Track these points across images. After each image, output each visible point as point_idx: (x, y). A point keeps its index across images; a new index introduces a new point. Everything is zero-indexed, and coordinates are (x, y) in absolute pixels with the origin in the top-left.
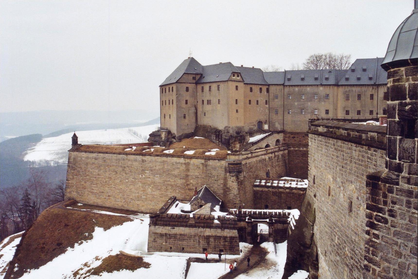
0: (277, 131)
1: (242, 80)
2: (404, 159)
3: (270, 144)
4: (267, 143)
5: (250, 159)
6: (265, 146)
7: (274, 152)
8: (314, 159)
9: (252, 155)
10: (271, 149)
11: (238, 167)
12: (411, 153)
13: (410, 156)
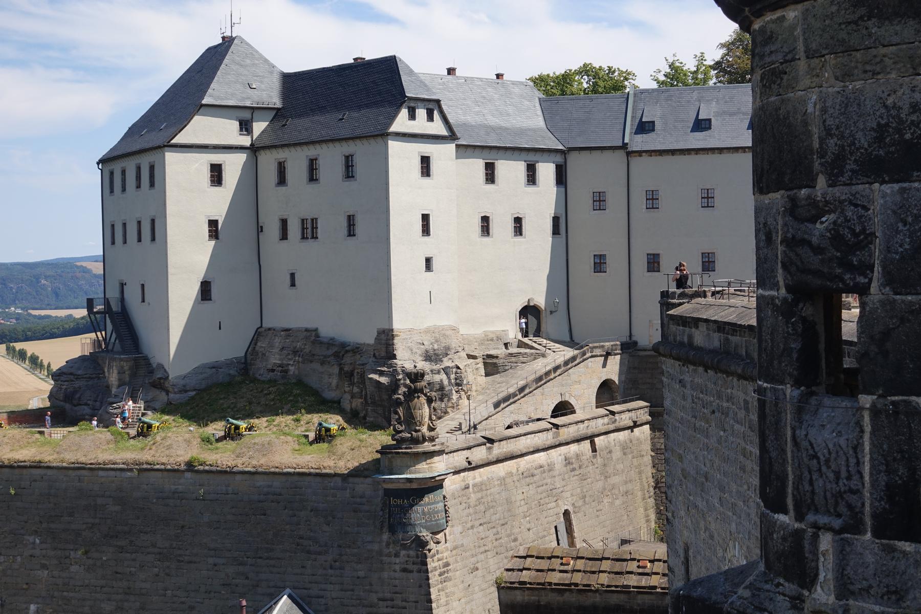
1: (444, 132)
2: (817, 511)
6: (553, 412)
7: (591, 438)
8: (683, 470)
9: (490, 448)
10: (577, 423)
12: (844, 474)
13: (840, 495)
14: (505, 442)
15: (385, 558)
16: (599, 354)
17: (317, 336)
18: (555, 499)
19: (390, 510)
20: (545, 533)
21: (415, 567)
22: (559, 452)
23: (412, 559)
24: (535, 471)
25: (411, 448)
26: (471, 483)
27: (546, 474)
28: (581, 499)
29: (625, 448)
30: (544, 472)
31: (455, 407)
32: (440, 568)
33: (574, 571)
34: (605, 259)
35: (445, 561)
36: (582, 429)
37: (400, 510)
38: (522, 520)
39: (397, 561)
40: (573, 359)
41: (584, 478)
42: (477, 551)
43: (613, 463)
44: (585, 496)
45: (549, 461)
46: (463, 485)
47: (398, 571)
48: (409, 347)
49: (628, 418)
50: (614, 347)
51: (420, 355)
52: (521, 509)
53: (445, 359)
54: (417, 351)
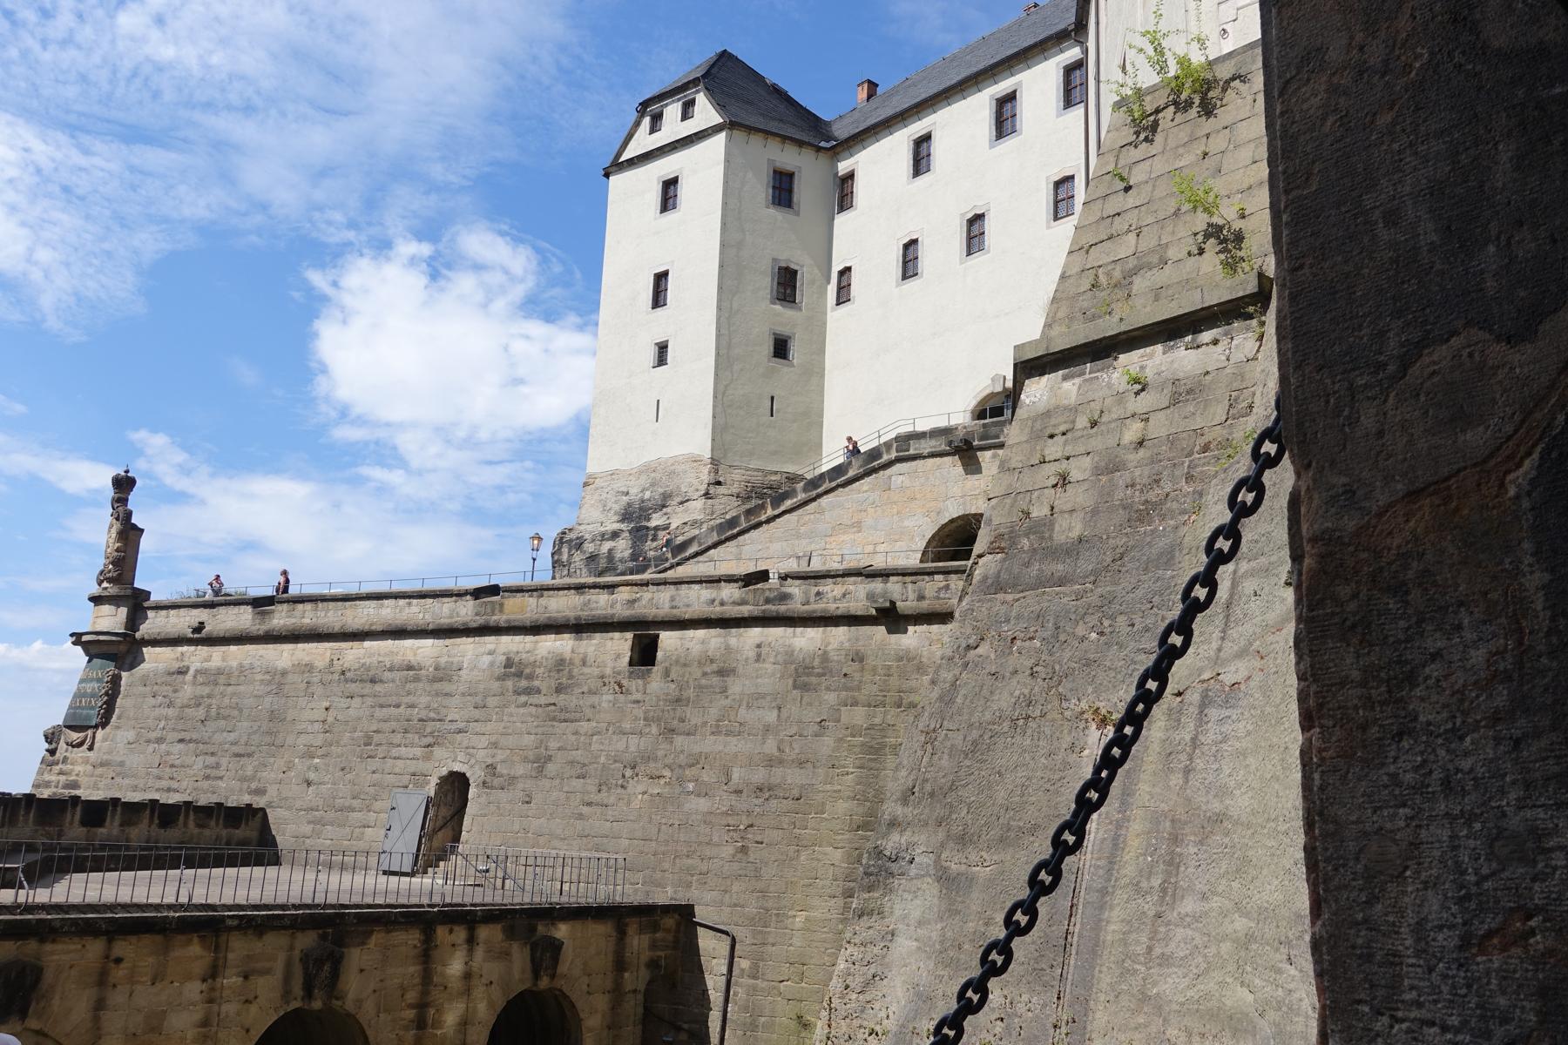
14: (308, 606)
18: (430, 740)
20: (356, 803)
24: (388, 675)
27: (421, 685)
28: (525, 760)
30: (417, 679)
38: (297, 760)
44: (549, 758)
45: (443, 660)
46: (176, 665)
52: (303, 739)
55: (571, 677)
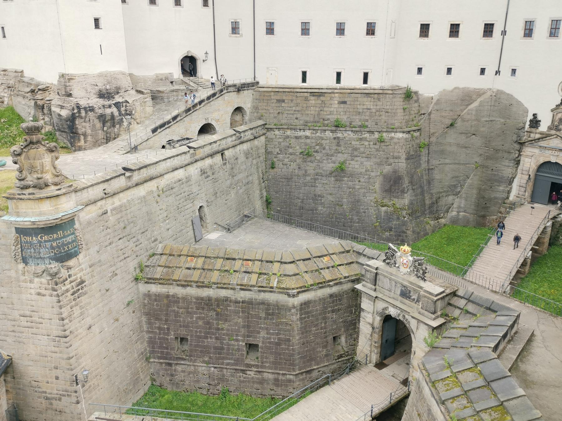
0: (234, 86)
3: (213, 123)
4: (204, 122)
5: (121, 195)
11: (57, 239)
14: (145, 169)
15: (21, 284)
16: (232, 91)
17: (22, 76)
18: (192, 201)
19: (21, 245)
20: (183, 228)
21: (48, 292)
22: (196, 167)
23: (44, 286)
24: (175, 185)
25: (34, 194)
26: (109, 208)
27: (184, 185)
28: (213, 195)
29: (247, 154)
30: (183, 183)
31: (128, 130)
32: (73, 288)
33: (194, 269)
34: (239, 25)
35: (79, 280)
36: (215, 147)
37: (30, 247)
38: (162, 224)
39: (32, 286)
40: (214, 95)
41: (216, 180)
42: (116, 260)
43: (238, 166)
44: (217, 193)
45: (187, 175)
46: (100, 212)
47: (34, 294)
48: (84, 88)
49: (250, 134)
50: (243, 86)
51: (94, 94)
52: (160, 217)
53: (116, 97)
54: (92, 90)
55: (214, 170)
